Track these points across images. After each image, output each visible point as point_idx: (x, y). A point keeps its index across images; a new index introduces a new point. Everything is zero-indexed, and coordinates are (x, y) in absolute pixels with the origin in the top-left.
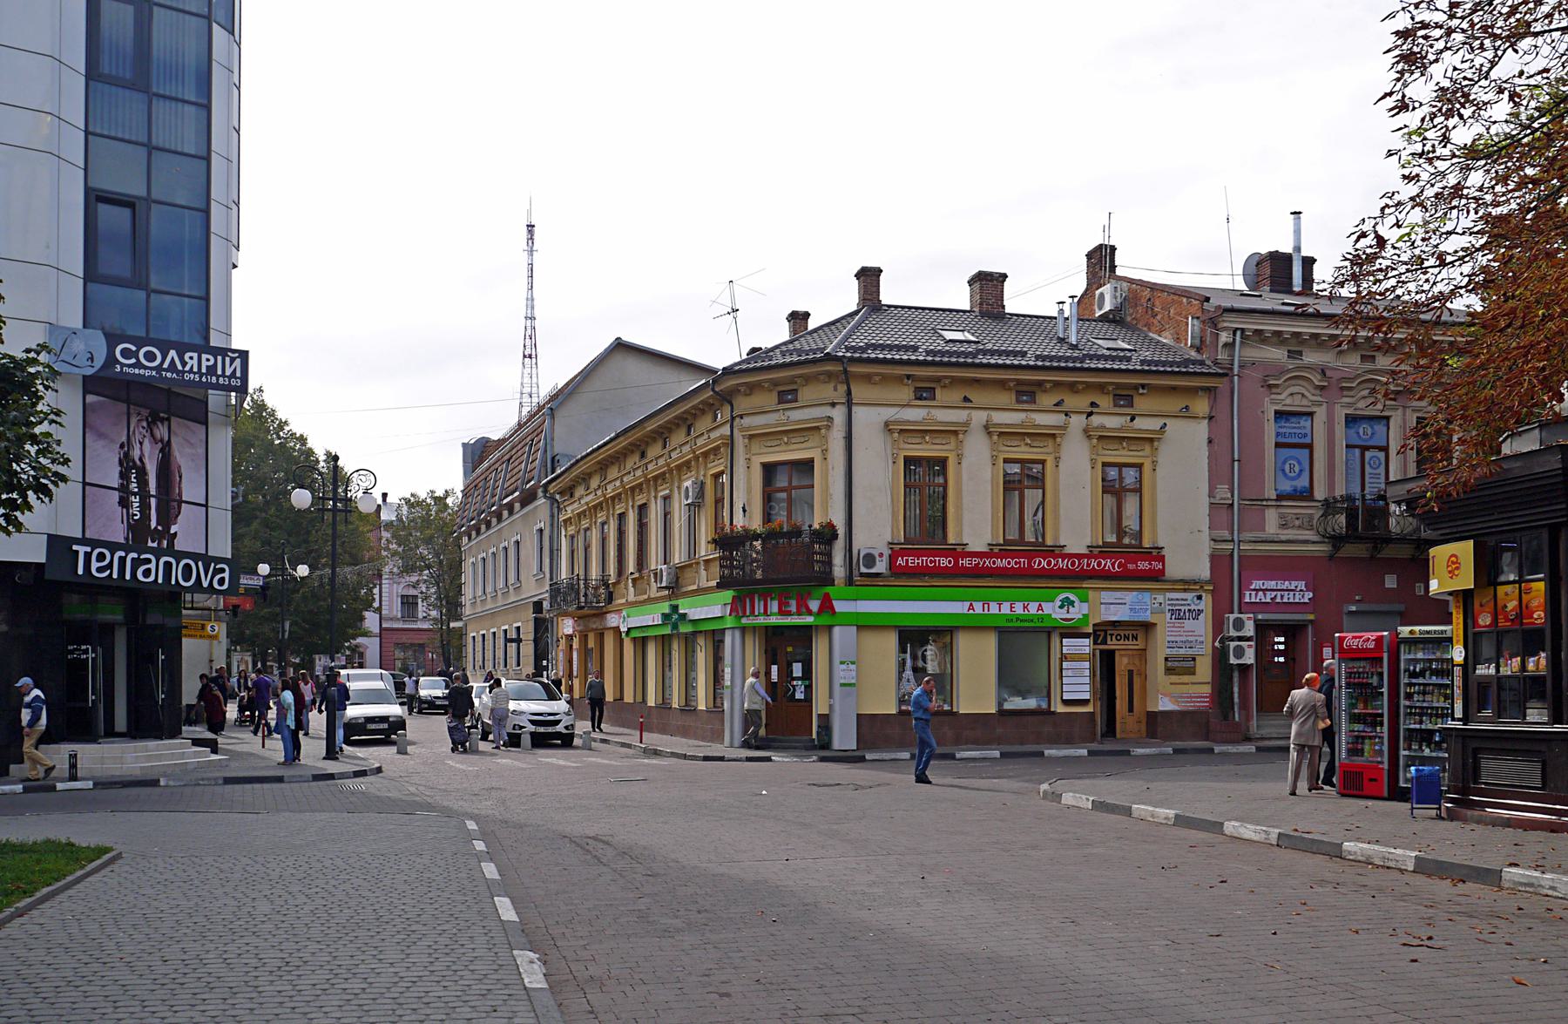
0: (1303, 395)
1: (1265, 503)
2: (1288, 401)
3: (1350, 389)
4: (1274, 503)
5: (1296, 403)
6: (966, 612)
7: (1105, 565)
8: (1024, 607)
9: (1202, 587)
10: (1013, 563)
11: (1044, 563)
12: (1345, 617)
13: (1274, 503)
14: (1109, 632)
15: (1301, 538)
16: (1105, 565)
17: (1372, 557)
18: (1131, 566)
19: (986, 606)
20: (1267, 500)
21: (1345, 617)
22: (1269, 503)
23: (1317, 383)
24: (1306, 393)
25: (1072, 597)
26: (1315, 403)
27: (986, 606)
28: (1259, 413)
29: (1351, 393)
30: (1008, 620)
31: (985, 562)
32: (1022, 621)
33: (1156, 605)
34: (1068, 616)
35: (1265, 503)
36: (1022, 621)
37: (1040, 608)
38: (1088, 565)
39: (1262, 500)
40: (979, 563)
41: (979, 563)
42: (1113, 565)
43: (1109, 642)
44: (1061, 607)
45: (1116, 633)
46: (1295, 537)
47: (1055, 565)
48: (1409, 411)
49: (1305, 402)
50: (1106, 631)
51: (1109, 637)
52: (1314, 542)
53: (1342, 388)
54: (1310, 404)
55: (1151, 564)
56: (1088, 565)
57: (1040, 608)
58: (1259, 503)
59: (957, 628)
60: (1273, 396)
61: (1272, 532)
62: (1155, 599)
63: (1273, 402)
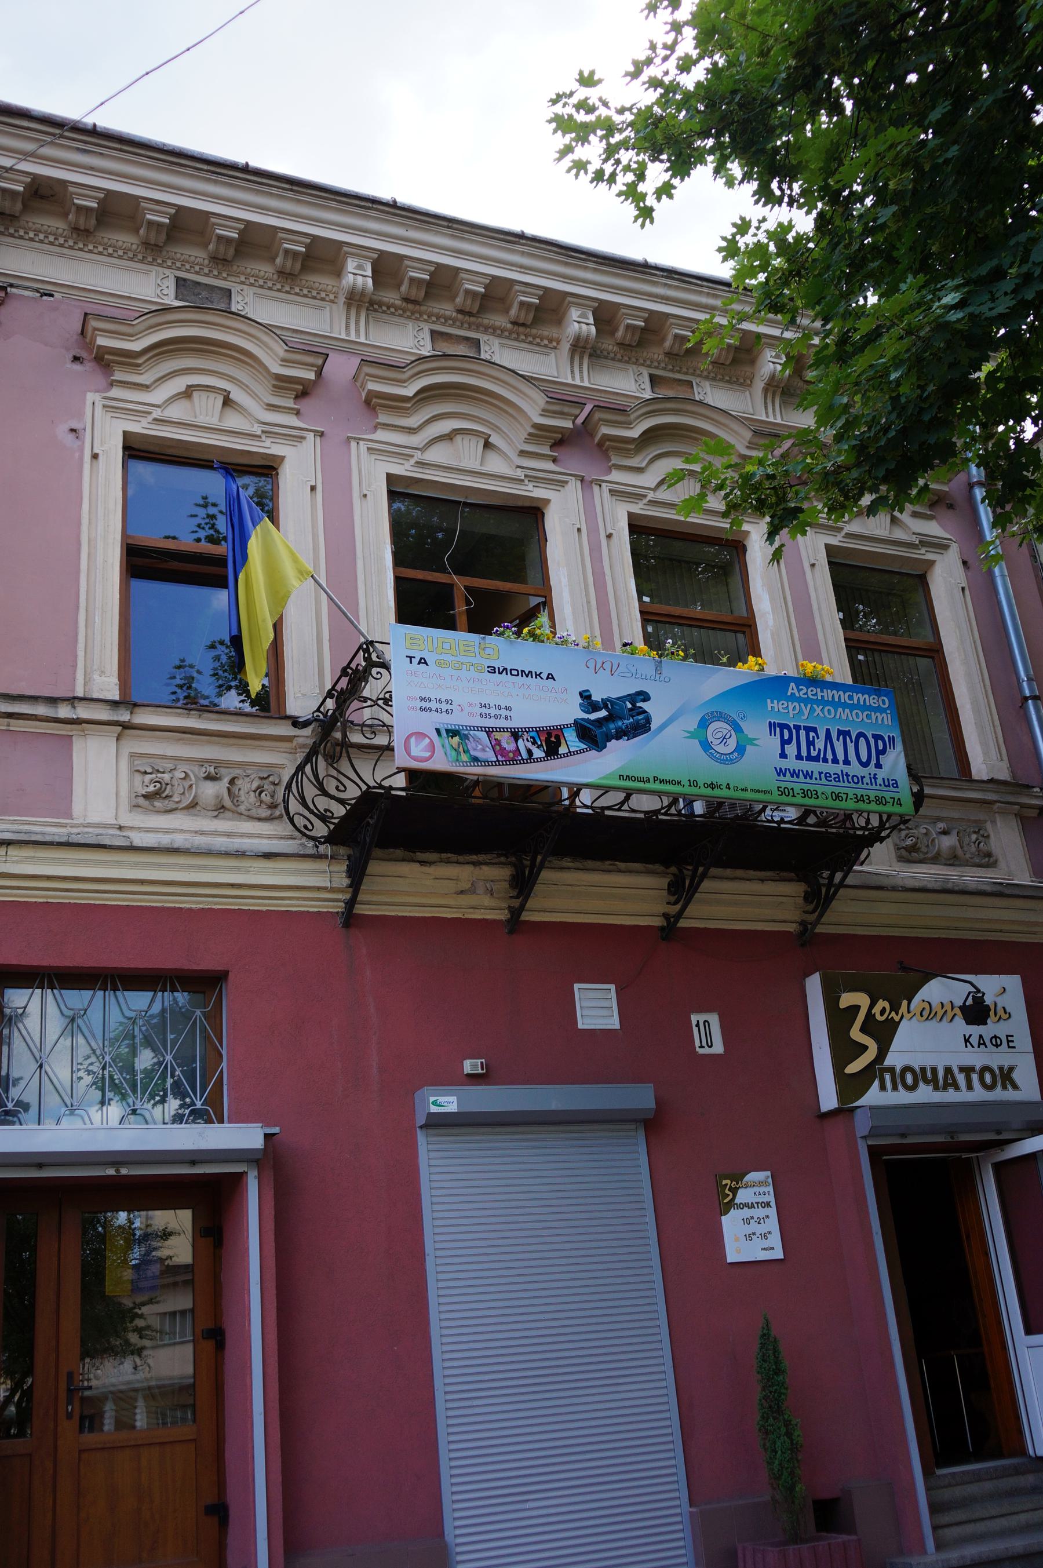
0: (227, 402)
1: (64, 712)
2: (177, 412)
3: (397, 404)
4: (103, 714)
5: (202, 420)
12: (421, 1138)
13: (103, 714)
15: (220, 843)
17: (515, 923)
20: (73, 701)
21: (418, 1131)
22: (83, 712)
23: (277, 369)
24: (236, 395)
26: (270, 431)
28: (62, 430)
29: (413, 421)
35: (64, 712)
39: (53, 701)
46: (200, 841)
48: (601, 496)
49: (233, 421)
52: (268, 856)
53: (372, 403)
54: (257, 430)
58: (41, 710)
60: (116, 392)
61: (94, 818)
63: (112, 408)
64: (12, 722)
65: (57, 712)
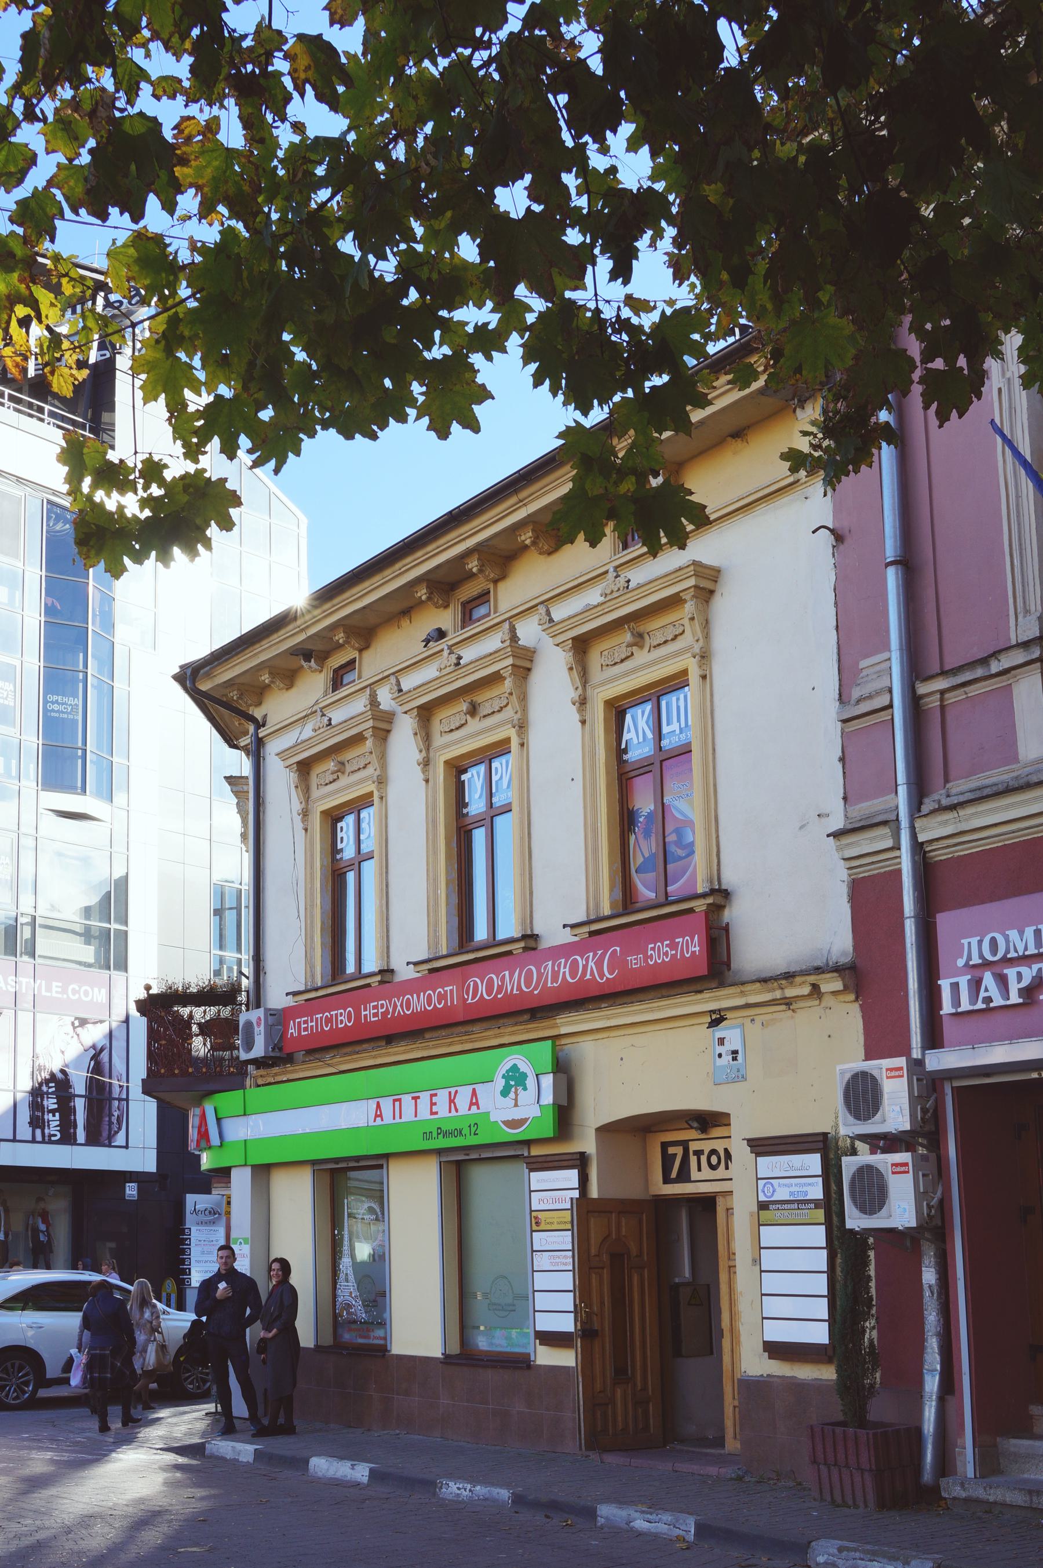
6: (371, 1123)
7: (585, 967)
8: (452, 1101)
9: (815, 987)
10: (435, 999)
11: (482, 989)
14: (693, 1146)
16: (585, 967)
18: (634, 961)
19: (397, 1104)
25: (524, 1067)
27: (397, 1104)
30: (427, 1136)
31: (395, 1006)
32: (446, 1134)
33: (727, 1059)
34: (517, 1114)
36: (446, 1134)
37: (474, 1102)
38: (555, 975)
40: (387, 1011)
41: (387, 1011)
42: (599, 964)
43: (695, 1175)
44: (505, 1093)
45: (706, 1146)
47: (499, 991)
50: (685, 1144)
51: (693, 1160)
55: (673, 946)
56: (555, 975)
57: (474, 1102)
59: (387, 1156)
62: (721, 1041)
64: (966, 689)
65: (989, 670)
